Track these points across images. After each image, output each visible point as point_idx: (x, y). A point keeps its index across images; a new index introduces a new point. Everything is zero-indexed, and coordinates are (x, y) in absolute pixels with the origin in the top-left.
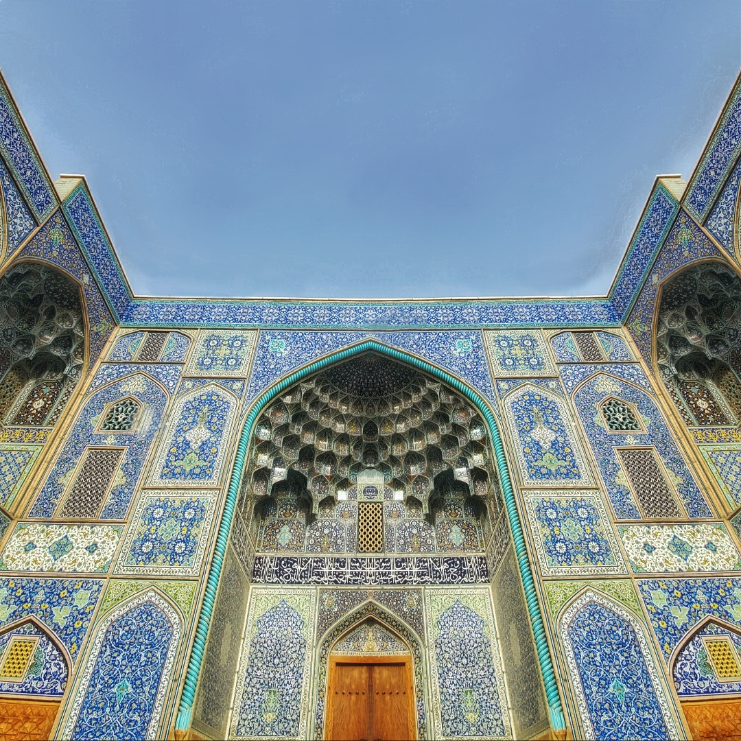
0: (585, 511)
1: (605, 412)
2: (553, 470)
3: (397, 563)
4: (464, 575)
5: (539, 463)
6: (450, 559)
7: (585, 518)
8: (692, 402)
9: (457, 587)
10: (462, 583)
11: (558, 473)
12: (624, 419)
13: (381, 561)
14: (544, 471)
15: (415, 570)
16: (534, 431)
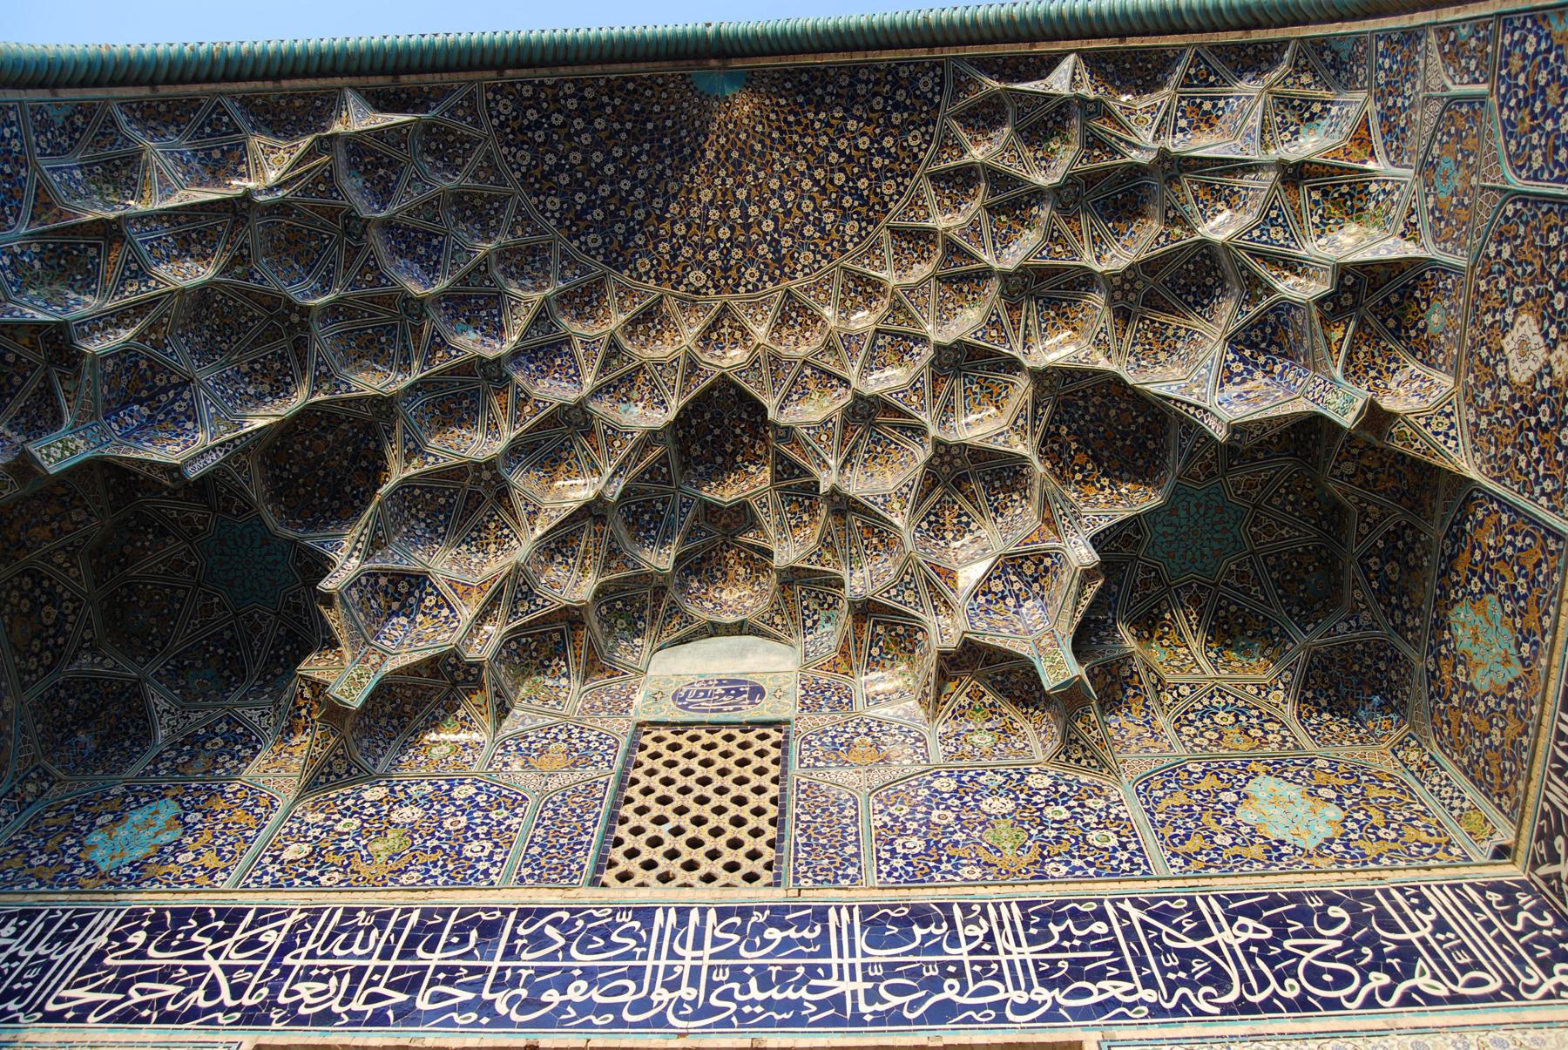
9: (1378, 1023)
13: (758, 918)
15: (1028, 952)
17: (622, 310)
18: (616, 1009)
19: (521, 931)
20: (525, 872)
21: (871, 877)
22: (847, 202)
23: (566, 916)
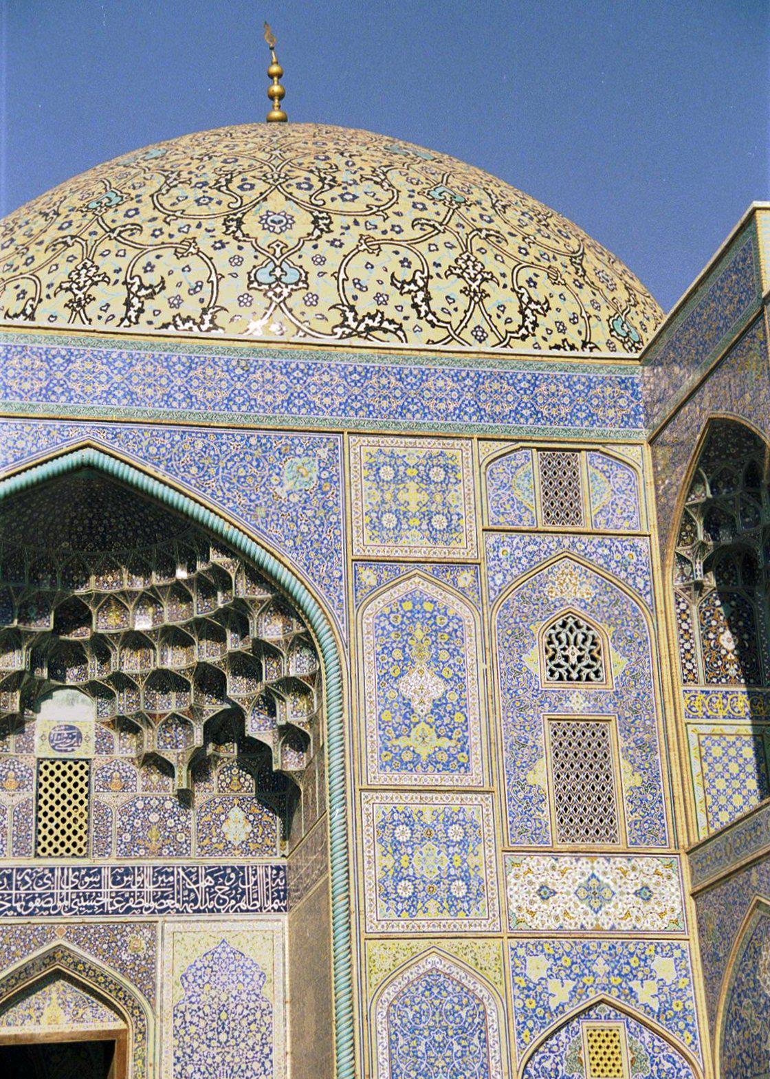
0: (461, 830)
1: (550, 643)
2: (424, 757)
3: (114, 876)
4: (241, 899)
5: (403, 742)
6: (220, 870)
7: (457, 842)
8: (711, 636)
9: (226, 918)
10: (236, 911)
11: (432, 761)
12: (580, 659)
13: (83, 872)
14: (407, 757)
15: (149, 888)
16: (406, 676)
17: (30, 560)
18: (48, 909)
19: (19, 878)
20: (15, 849)
21: (114, 854)
22: (140, 532)
23: (29, 871)
